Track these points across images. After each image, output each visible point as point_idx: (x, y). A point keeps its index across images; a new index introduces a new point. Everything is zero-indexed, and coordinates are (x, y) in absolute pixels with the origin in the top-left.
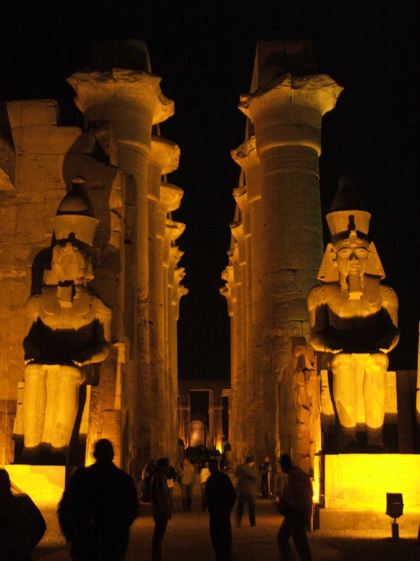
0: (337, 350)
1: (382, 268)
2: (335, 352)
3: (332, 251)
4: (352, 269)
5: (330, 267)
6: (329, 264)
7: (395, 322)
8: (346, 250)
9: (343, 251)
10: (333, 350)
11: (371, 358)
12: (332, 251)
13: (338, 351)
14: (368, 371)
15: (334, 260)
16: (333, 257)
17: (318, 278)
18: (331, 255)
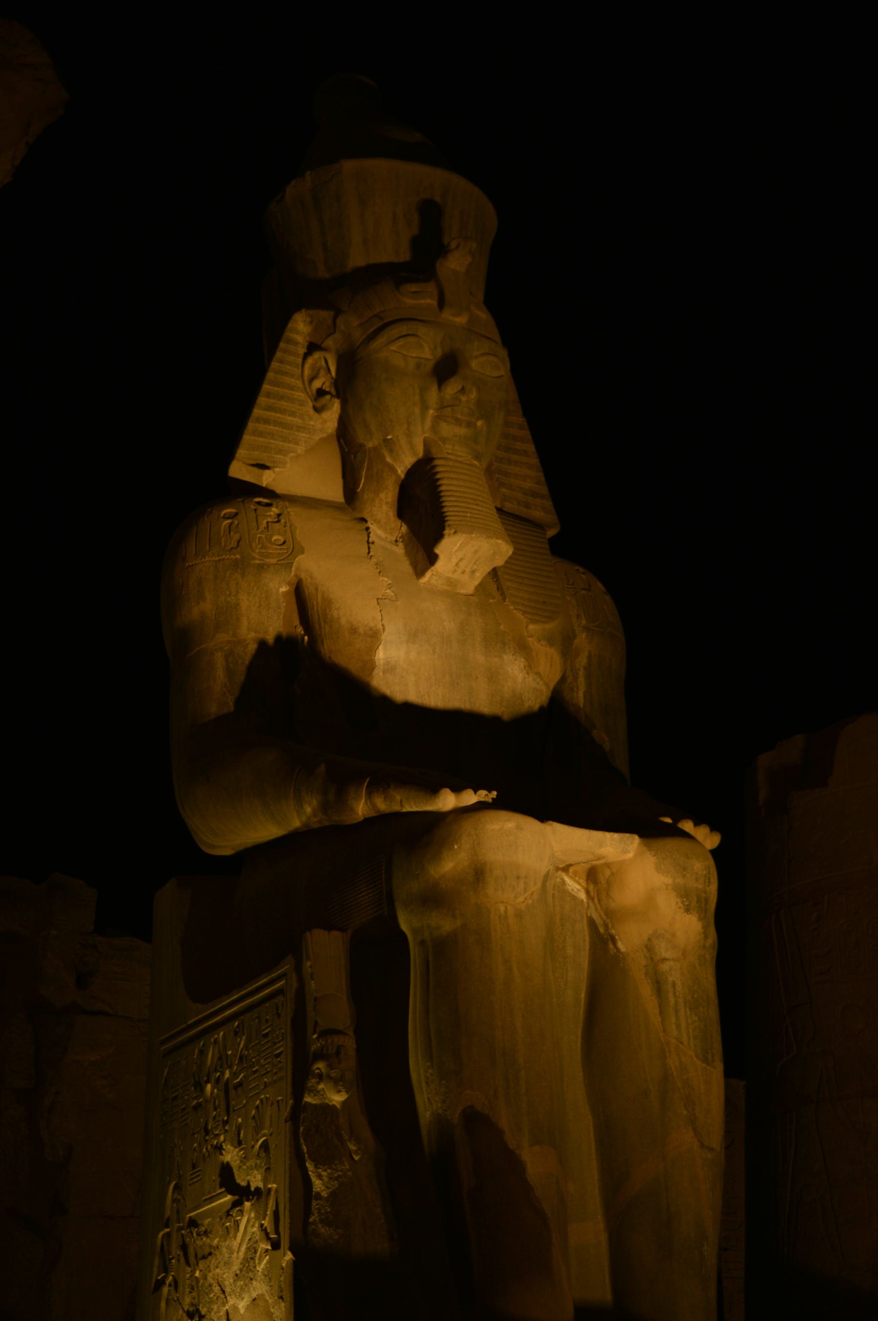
0: (457, 789)
1: (544, 490)
2: (448, 801)
3: (312, 348)
4: (447, 430)
5: (300, 428)
6: (293, 414)
7: (621, 762)
8: (422, 330)
9: (403, 329)
10: (434, 790)
11: (649, 861)
12: (312, 348)
13: (470, 798)
14: (629, 939)
15: (321, 393)
16: (317, 384)
17: (238, 470)
18: (307, 372)
